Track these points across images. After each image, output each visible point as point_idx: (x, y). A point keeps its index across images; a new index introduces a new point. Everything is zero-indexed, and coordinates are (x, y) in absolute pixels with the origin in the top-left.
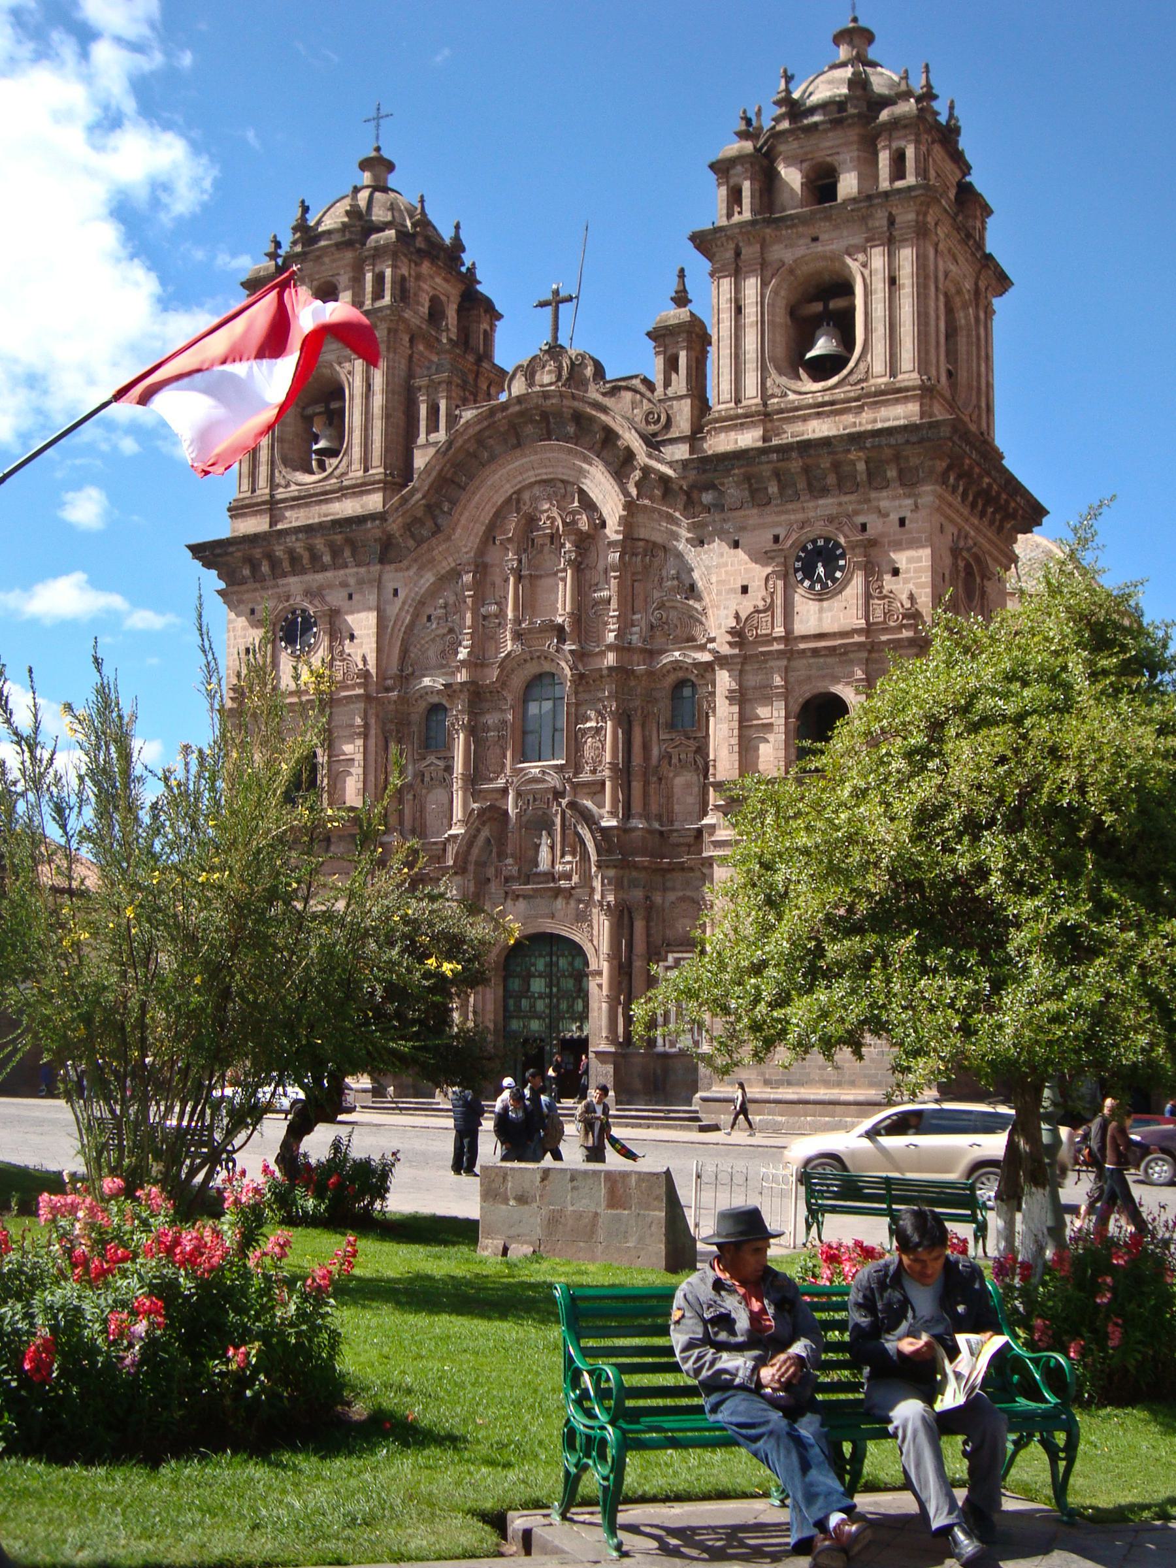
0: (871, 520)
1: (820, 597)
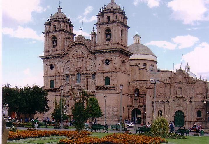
0: (112, 58)
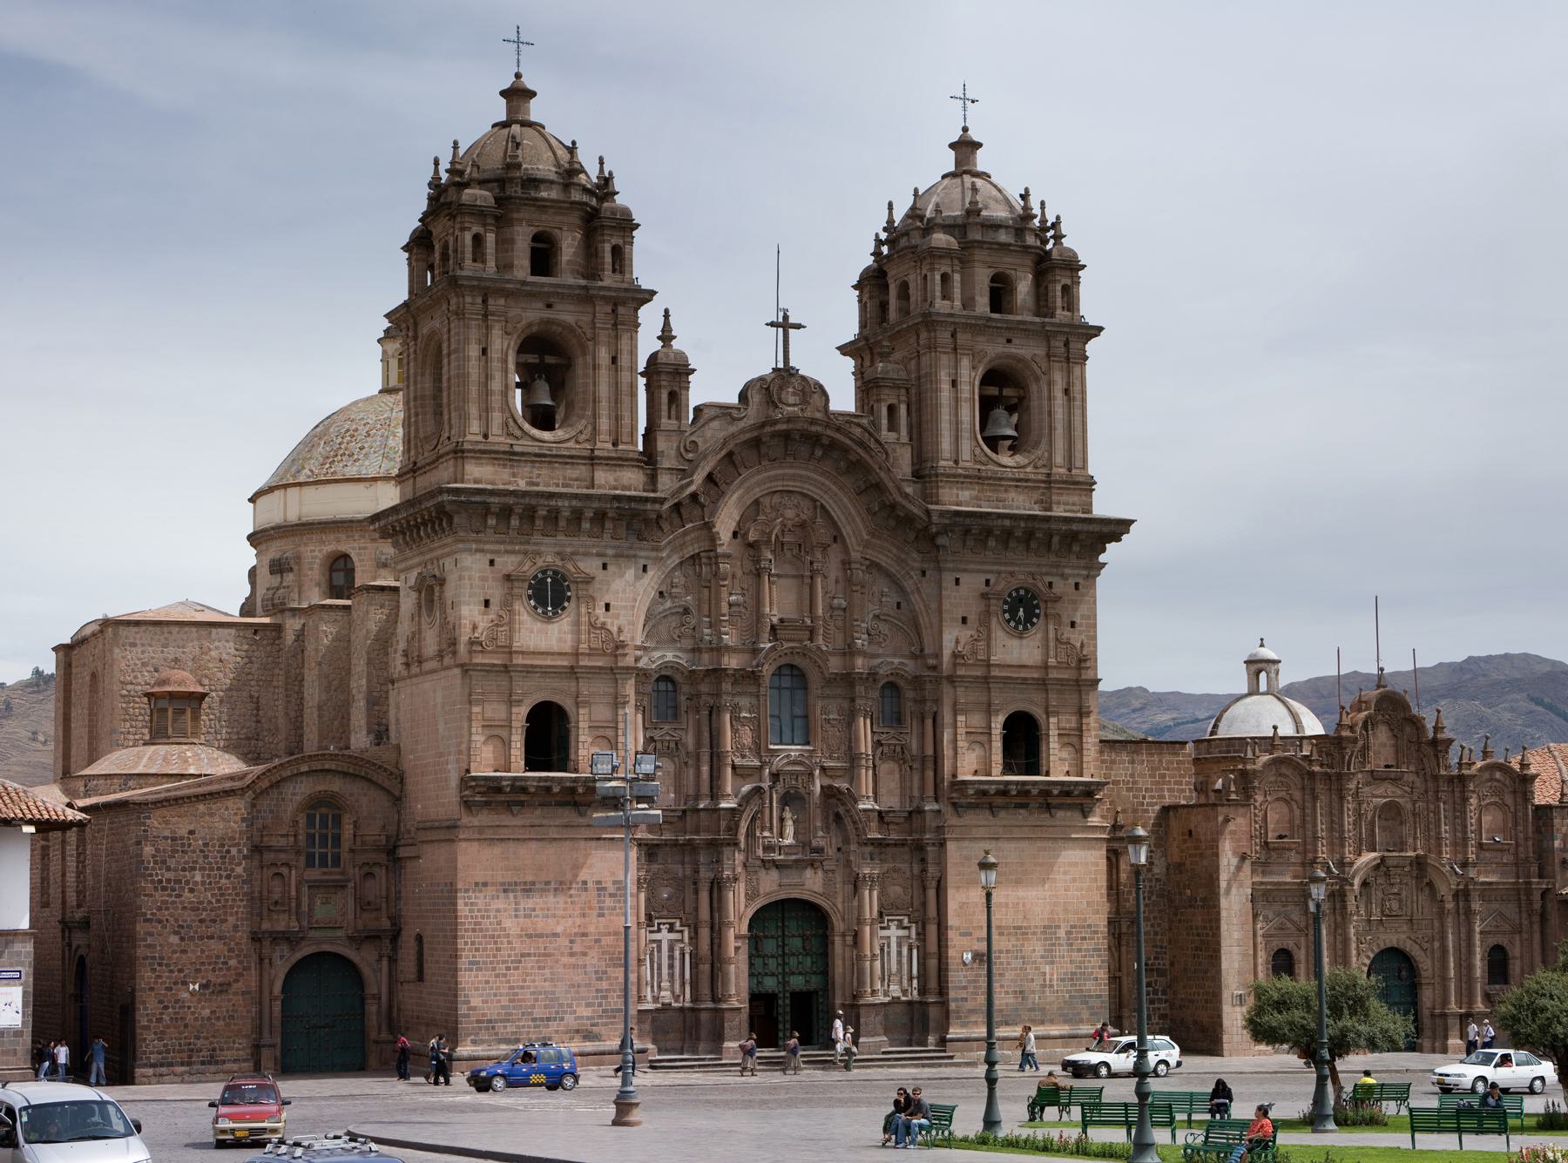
0: (1056, 581)
1: (1021, 638)
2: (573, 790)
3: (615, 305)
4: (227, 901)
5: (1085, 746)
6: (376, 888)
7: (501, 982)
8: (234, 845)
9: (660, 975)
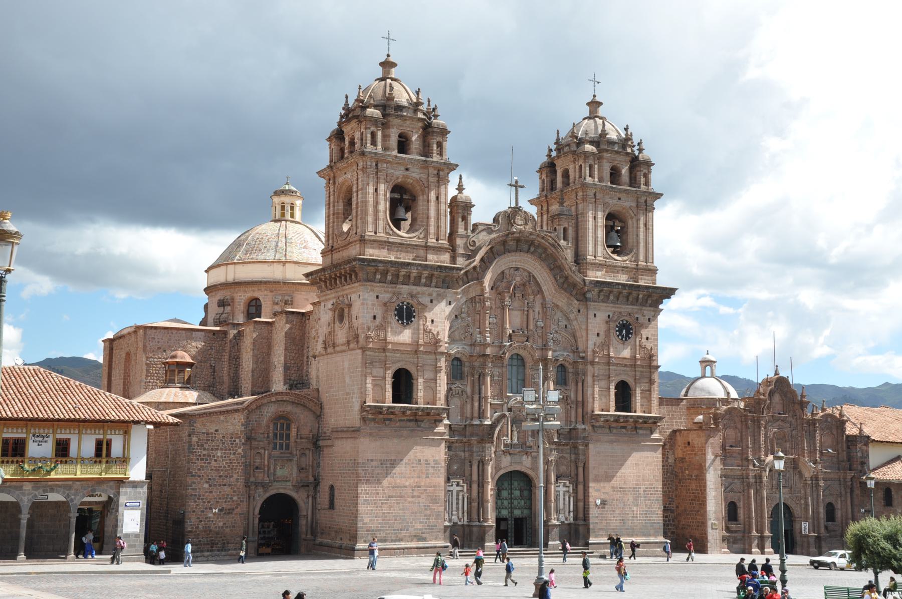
0: (639, 316)
2: (415, 414)
3: (439, 171)
4: (233, 466)
5: (652, 399)
6: (308, 460)
7: (379, 510)
8: (238, 438)
9: (452, 508)
